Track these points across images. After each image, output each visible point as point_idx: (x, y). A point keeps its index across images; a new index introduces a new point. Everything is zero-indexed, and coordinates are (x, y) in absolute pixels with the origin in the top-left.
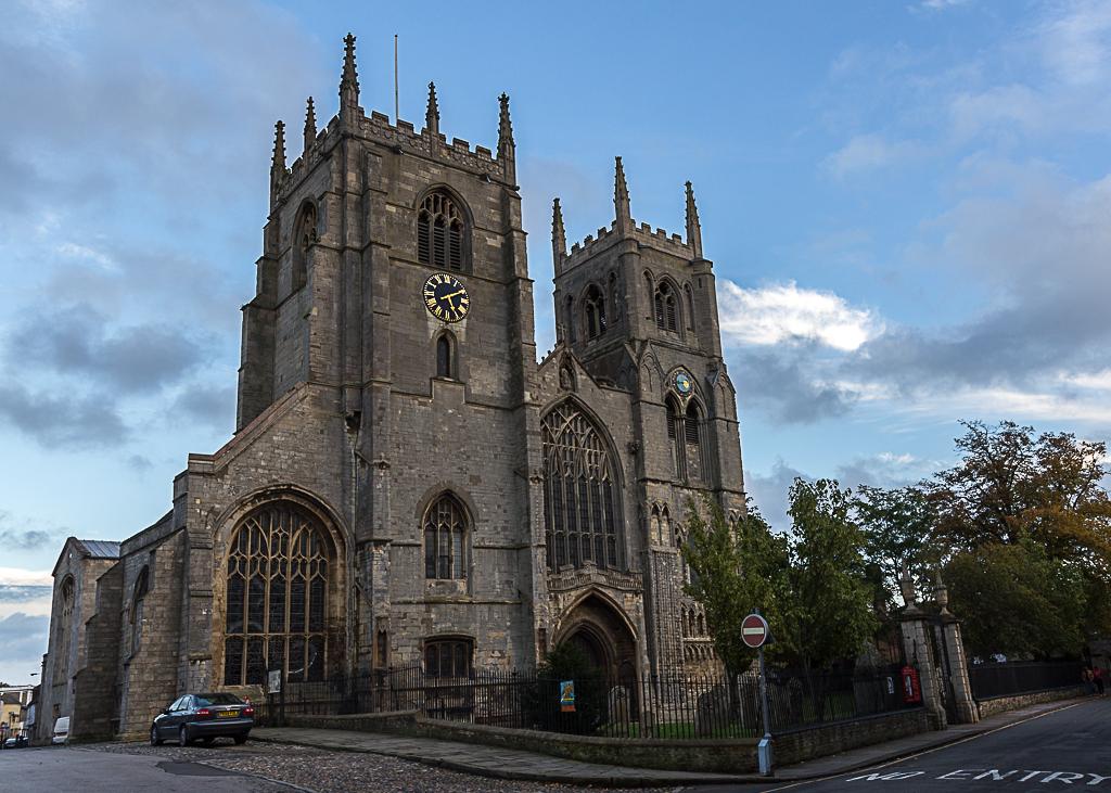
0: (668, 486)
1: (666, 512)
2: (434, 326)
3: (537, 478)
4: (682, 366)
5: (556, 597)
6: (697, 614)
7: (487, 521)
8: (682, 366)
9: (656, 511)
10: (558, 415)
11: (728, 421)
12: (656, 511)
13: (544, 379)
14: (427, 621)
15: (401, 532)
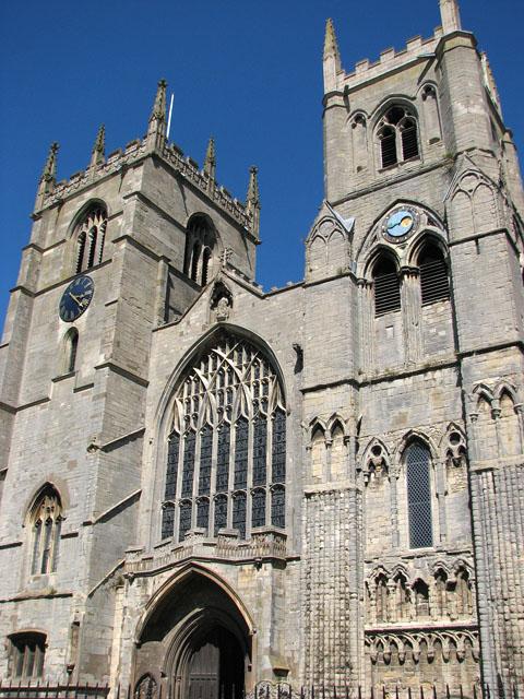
0: (340, 389)
1: (337, 426)
2: (64, 327)
3: (92, 447)
4: (399, 201)
5: (145, 582)
6: (410, 581)
7: (76, 505)
8: (399, 201)
9: (317, 429)
10: (216, 354)
11: (476, 239)
12: (317, 429)
13: (188, 323)
14: (14, 619)
15: (10, 535)
